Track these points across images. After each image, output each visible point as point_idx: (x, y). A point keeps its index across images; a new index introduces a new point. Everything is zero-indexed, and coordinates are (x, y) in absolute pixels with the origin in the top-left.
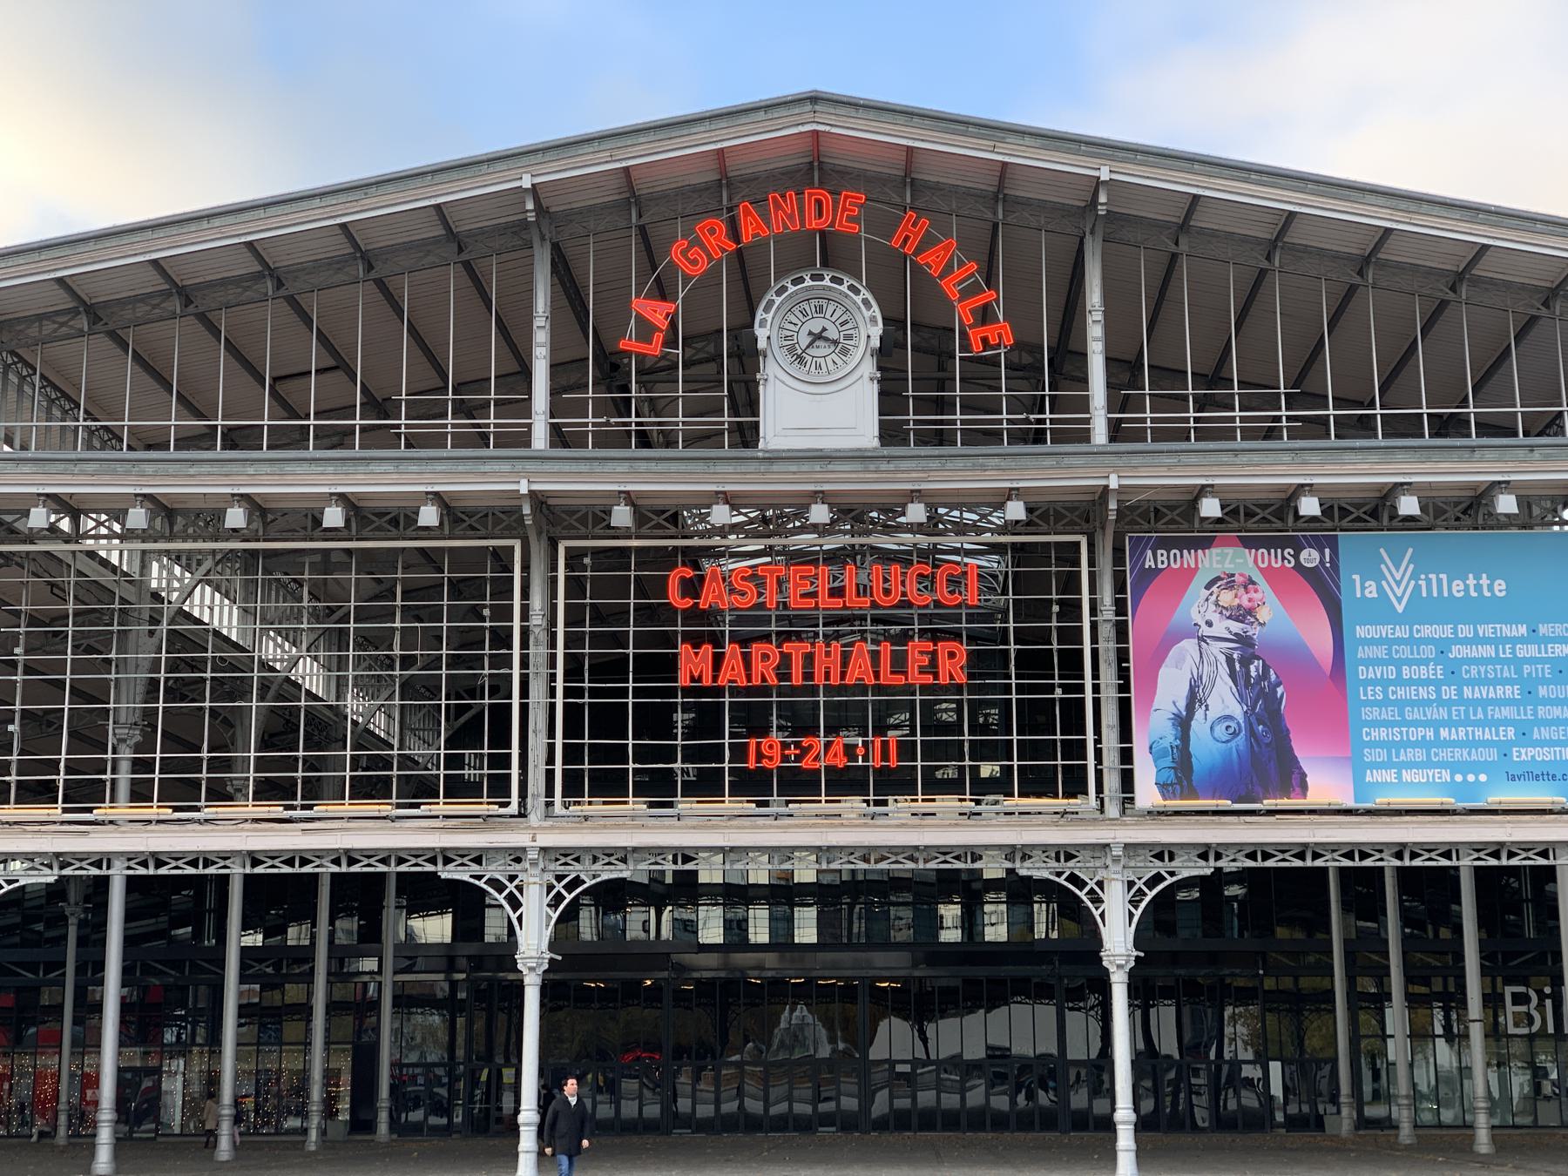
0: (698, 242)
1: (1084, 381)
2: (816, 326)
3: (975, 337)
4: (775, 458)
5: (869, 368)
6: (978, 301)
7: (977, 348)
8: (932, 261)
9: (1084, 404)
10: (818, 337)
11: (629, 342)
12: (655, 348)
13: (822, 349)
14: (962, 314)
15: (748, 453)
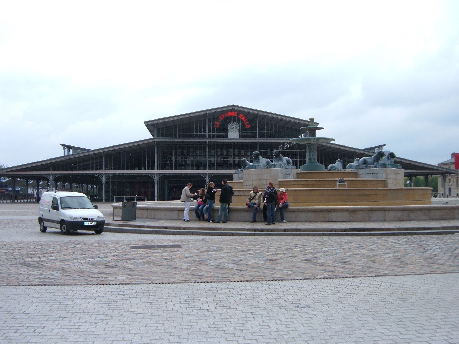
0: (221, 116)
1: (256, 131)
2: (233, 127)
3: (247, 126)
4: (230, 139)
5: (238, 131)
6: (247, 123)
7: (247, 127)
8: (242, 119)
9: (256, 133)
10: (234, 128)
11: (215, 126)
12: (218, 127)
13: (234, 129)
14: (246, 124)
15: (227, 138)
